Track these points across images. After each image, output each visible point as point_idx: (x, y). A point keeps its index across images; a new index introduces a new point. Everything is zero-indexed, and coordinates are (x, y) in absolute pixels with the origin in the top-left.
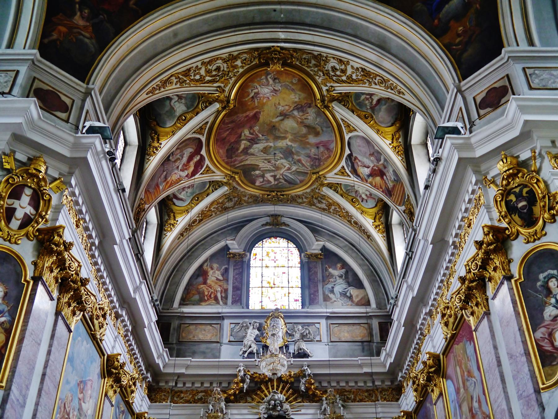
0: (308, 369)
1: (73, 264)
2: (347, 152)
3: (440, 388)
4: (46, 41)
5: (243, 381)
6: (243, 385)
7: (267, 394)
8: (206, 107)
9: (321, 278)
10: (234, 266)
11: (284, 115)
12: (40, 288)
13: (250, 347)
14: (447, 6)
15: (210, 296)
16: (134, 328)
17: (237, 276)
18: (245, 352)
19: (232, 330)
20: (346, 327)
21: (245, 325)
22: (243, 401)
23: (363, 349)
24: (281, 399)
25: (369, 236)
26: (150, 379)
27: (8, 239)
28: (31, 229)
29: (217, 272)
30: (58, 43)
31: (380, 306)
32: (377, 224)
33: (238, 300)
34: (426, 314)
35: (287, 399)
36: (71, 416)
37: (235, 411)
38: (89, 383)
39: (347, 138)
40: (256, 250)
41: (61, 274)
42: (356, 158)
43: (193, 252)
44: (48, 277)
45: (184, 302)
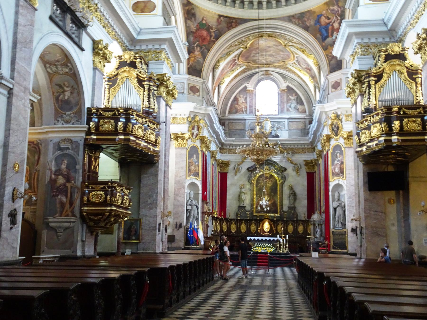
2: (296, 59)
4: (189, 66)
8: (237, 50)
15: (240, 110)
16: (217, 137)
19: (250, 125)
23: (301, 133)
25: (307, 84)
28: (198, 137)
39: (296, 56)
40: (258, 87)
45: (230, 113)
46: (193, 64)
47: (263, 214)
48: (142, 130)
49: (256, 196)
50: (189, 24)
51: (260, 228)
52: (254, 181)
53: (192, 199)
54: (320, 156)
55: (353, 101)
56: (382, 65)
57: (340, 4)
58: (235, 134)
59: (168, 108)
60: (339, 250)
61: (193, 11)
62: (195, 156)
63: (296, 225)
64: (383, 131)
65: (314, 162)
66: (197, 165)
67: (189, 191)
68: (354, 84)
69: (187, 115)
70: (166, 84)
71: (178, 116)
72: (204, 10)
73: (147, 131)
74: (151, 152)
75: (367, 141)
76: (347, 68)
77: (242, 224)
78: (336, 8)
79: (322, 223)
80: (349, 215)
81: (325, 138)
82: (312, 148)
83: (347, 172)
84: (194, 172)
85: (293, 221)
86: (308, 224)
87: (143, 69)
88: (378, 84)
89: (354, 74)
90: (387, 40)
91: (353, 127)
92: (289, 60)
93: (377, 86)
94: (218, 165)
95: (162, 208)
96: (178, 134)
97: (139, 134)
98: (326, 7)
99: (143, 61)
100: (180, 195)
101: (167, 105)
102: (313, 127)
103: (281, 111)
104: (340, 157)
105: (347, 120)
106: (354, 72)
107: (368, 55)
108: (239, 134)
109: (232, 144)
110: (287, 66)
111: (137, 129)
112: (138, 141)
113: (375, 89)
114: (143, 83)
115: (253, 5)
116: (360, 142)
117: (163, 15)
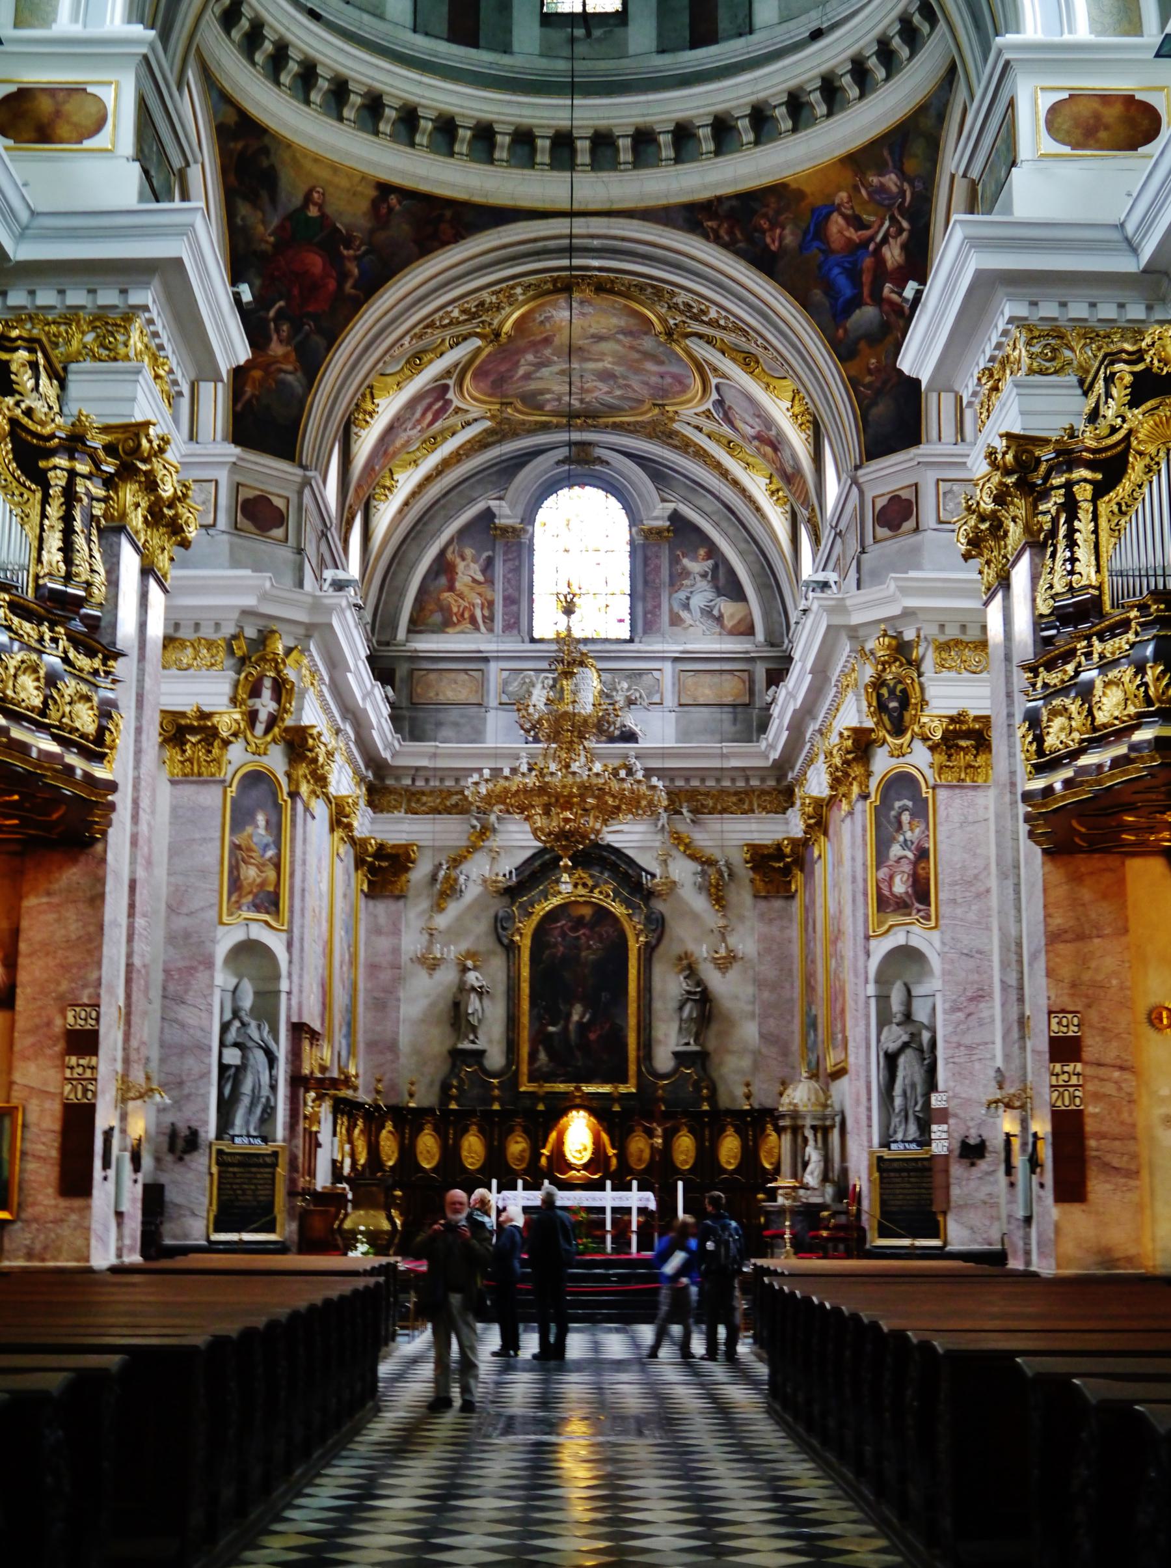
2: (715, 396)
4: (239, 407)
8: (457, 344)
9: (667, 580)
10: (505, 553)
11: (600, 338)
14: (858, 311)
15: (462, 615)
17: (510, 576)
19: (506, 683)
20: (708, 677)
21: (527, 680)
23: (735, 721)
28: (276, 730)
29: (472, 565)
30: (254, 402)
31: (773, 641)
32: (773, 487)
37: (512, 827)
39: (714, 381)
40: (542, 515)
42: (730, 408)
43: (425, 524)
44: (304, 789)
46: (258, 398)
47: (561, 1087)
48: (38, 680)
50: (243, 219)
51: (549, 1146)
52: (521, 935)
53: (246, 1019)
54: (818, 823)
55: (990, 574)
56: (1124, 421)
57: (911, 166)
58: (439, 724)
59: (152, 584)
60: (906, 1242)
61: (265, 163)
62: (261, 819)
64: (1148, 701)
65: (788, 850)
66: (270, 859)
67: (234, 981)
68: (1000, 498)
69: (229, 630)
70: (146, 473)
71: (186, 633)
72: (317, 160)
73: (60, 685)
74: (75, 784)
75: (1074, 746)
76: (940, 439)
77: (465, 1131)
78: (891, 180)
79: (828, 1123)
80: (952, 1084)
81: (849, 743)
82: (780, 792)
83: (943, 896)
84: (255, 890)
86: (763, 1130)
87: (43, 397)
88: (1106, 498)
89: (1005, 453)
90: (1136, 312)
91: (993, 697)
92: (688, 396)
93: (1103, 508)
94: (359, 862)
95: (119, 1054)
96: (183, 714)
97: (23, 695)
98: (848, 177)
99: (42, 361)
100: (189, 998)
101: (147, 571)
102: (791, 695)
104: (912, 830)
105: (941, 666)
106: (1000, 444)
107: (1056, 372)
108: (456, 724)
109: (425, 768)
110: (676, 426)
111: (12, 671)
112: (17, 733)
113: (1095, 518)
114: (42, 464)
115: (533, 150)
116: (1040, 752)
117: (140, 156)
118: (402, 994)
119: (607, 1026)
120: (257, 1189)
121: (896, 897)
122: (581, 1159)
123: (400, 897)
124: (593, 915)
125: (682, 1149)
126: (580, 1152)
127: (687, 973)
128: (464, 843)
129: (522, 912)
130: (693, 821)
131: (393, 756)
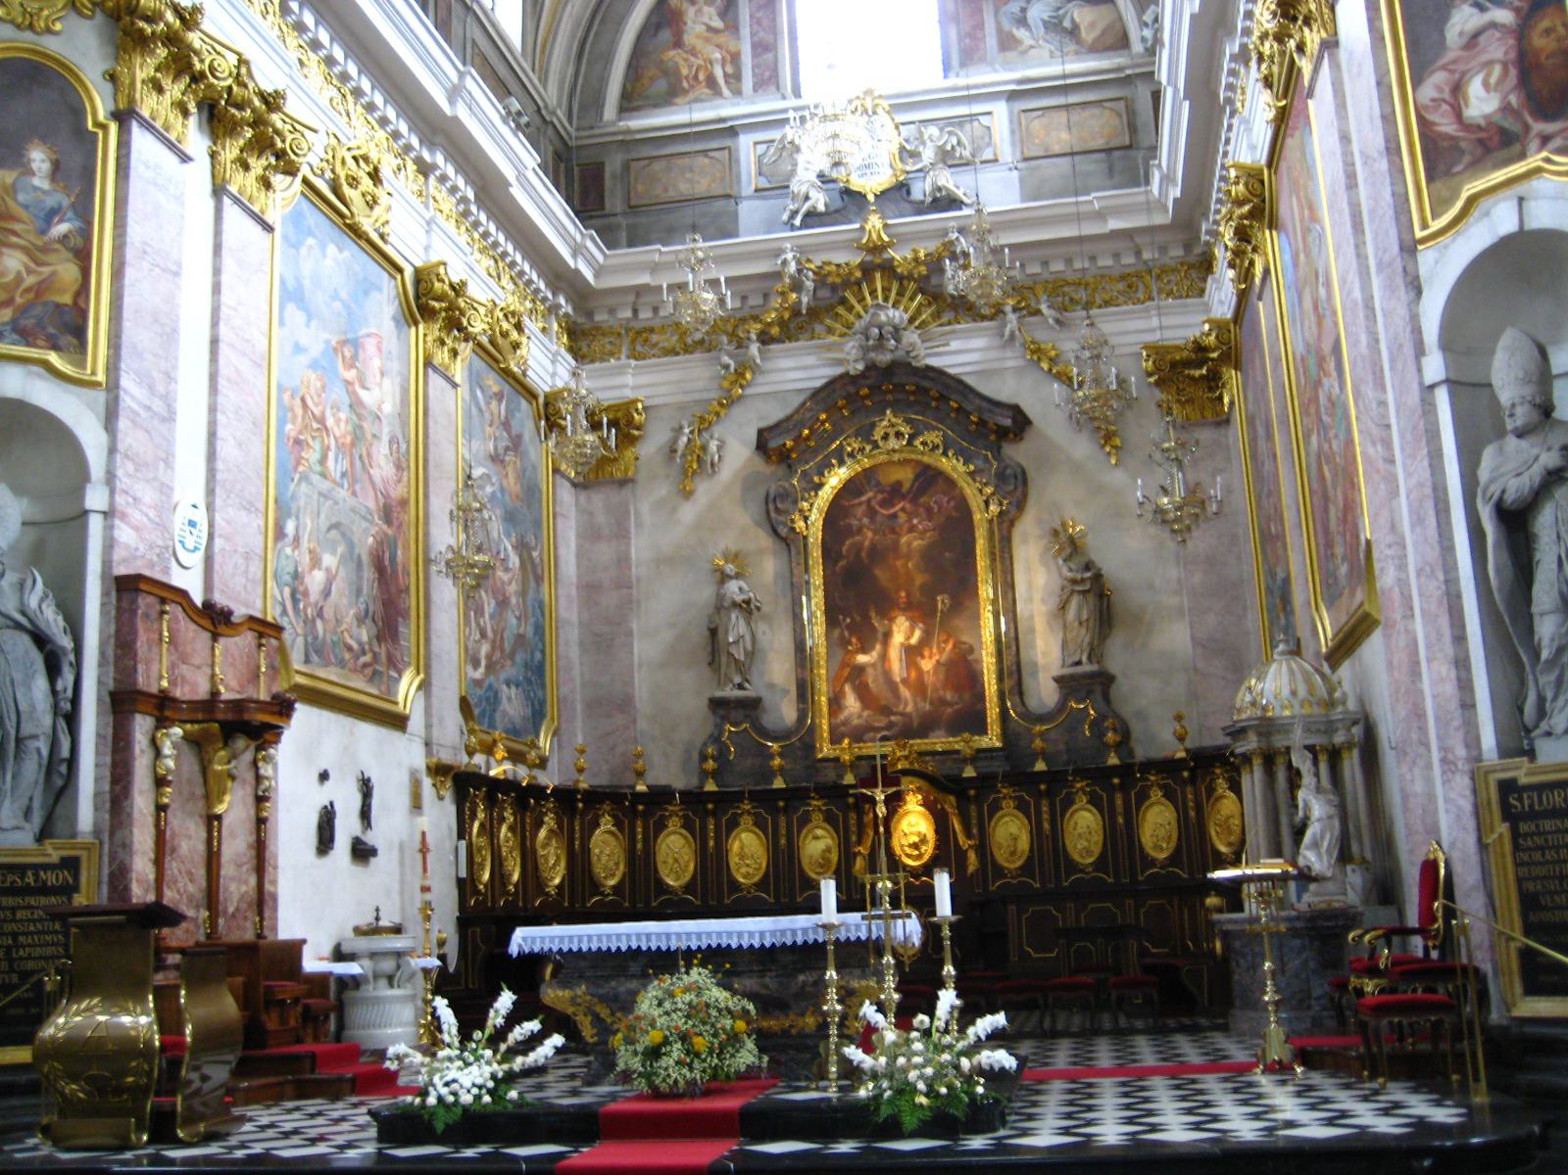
0: (962, 239)
1: (219, 60)
3: (1266, 254)
5: (797, 286)
6: (799, 298)
7: (862, 313)
12: (140, 138)
13: (807, 198)
15: (696, 77)
18: (794, 213)
19: (759, 159)
20: (1062, 116)
22: (806, 336)
23: (1111, 171)
24: (897, 321)
26: (566, 308)
27: (27, 23)
29: (706, 9)
33: (770, 78)
34: (1234, 58)
35: (911, 320)
36: (330, 422)
38: (370, 346)
41: (195, 92)
49: (831, 621)
52: (806, 519)
54: (1256, 214)
62: (39, 158)
63: (1119, 801)
66: (65, 238)
77: (733, 824)
79: (1339, 738)
82: (1191, 267)
84: (19, 300)
85: (1099, 776)
86: (1211, 790)
103: (965, 52)
118: (635, 627)
119: (950, 646)
120: (18, 946)
121: (1479, 127)
122: (920, 857)
123: (624, 482)
124: (917, 477)
125: (1079, 830)
126: (915, 846)
127: (1068, 551)
128: (714, 395)
129: (804, 485)
130: (1058, 321)
131: (597, 275)
